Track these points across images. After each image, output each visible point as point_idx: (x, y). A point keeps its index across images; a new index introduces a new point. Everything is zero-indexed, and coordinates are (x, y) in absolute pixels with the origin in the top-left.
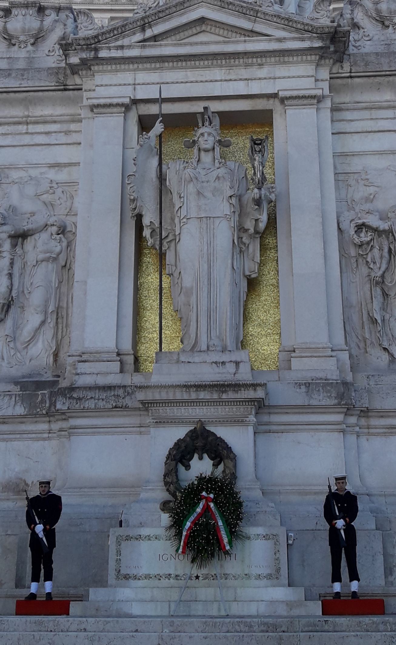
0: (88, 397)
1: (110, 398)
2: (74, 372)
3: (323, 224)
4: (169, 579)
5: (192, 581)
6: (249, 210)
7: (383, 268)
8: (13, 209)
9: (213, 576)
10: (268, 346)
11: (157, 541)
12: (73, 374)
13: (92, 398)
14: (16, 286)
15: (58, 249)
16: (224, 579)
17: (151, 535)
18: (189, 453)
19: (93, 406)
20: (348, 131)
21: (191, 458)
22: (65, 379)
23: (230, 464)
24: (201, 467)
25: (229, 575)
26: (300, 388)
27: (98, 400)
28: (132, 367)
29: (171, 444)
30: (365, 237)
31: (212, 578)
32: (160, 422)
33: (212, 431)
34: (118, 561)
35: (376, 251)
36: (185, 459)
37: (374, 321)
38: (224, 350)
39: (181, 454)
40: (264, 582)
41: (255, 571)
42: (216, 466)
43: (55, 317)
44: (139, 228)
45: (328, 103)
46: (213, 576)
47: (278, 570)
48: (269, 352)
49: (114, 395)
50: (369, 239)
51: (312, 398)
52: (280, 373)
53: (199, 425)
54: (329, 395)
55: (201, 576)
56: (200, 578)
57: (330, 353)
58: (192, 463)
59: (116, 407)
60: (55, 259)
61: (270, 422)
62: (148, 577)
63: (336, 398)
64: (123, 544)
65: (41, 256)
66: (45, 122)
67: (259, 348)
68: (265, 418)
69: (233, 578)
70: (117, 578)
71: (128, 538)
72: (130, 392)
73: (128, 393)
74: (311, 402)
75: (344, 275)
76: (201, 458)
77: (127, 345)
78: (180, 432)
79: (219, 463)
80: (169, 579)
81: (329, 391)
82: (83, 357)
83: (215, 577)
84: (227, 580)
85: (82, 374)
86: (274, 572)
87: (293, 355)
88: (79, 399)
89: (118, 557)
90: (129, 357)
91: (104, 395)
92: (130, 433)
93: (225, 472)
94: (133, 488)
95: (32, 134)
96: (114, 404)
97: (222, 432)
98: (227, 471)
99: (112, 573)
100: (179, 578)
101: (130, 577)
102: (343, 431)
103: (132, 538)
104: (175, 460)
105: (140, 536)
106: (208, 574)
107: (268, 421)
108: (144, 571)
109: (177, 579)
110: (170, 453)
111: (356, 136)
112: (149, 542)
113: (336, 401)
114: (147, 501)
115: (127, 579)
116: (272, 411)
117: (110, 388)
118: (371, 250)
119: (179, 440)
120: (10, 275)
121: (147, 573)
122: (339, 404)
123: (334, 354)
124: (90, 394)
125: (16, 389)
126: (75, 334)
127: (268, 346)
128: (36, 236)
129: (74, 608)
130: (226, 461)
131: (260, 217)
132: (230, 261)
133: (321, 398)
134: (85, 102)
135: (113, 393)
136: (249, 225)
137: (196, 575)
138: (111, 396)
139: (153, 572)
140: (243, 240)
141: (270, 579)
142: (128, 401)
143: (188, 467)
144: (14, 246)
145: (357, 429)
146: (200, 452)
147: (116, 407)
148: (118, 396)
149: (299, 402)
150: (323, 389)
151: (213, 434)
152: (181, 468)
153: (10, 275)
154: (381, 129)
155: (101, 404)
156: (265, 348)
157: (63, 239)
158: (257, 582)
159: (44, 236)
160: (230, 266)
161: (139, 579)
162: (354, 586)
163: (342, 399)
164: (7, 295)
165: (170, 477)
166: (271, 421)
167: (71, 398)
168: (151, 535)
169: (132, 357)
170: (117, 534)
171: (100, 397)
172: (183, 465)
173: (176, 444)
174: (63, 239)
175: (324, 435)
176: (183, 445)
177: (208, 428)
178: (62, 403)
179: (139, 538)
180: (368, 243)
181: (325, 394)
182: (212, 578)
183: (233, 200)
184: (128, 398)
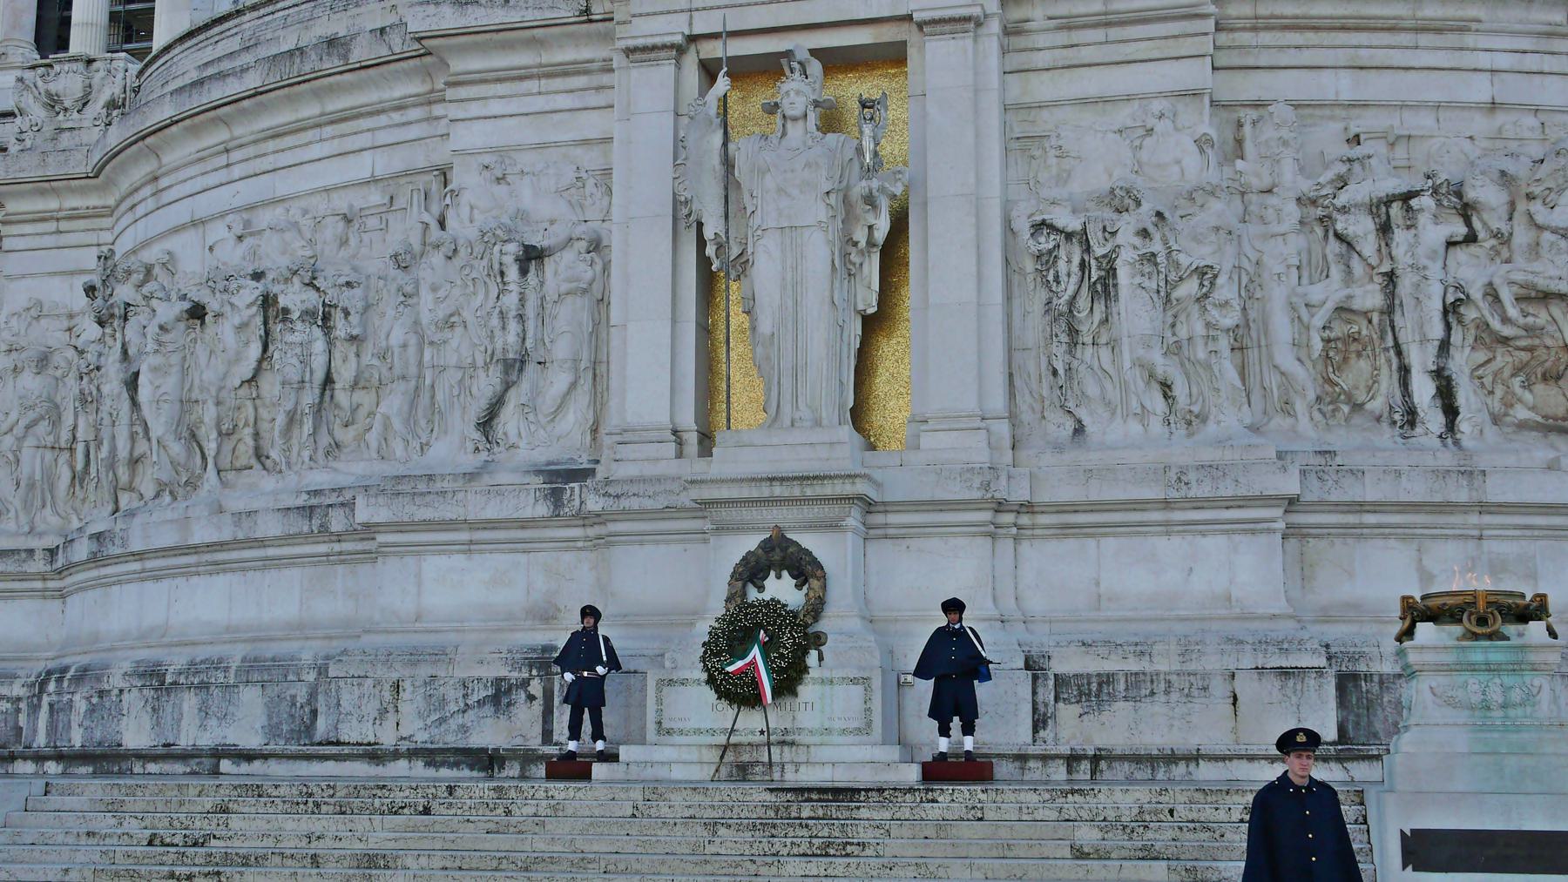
3: (978, 227)
6: (859, 211)
7: (1070, 292)
8: (521, 215)
14: (530, 334)
15: (589, 274)
20: (1032, 66)
24: (781, 589)
30: (1046, 242)
32: (722, 529)
35: (1062, 266)
37: (1055, 373)
38: (818, 423)
39: (752, 571)
40: (850, 739)
41: (838, 725)
42: (799, 587)
43: (590, 375)
44: (701, 243)
45: (995, 26)
47: (869, 724)
50: (1051, 246)
57: (978, 423)
60: (585, 291)
64: (666, 690)
65: (564, 287)
66: (566, 74)
68: (878, 519)
71: (671, 682)
75: (1016, 302)
76: (779, 577)
77: (687, 419)
78: (751, 542)
82: (626, 436)
88: (617, 496)
92: (690, 541)
95: (547, 93)
97: (807, 541)
99: (651, 727)
102: (993, 536)
108: (693, 724)
111: (1046, 76)
117: (659, 480)
118: (1055, 262)
120: (521, 318)
123: (983, 424)
124: (634, 489)
125: (537, 482)
126: (613, 403)
128: (557, 256)
129: (599, 770)
131: (872, 221)
132: (827, 293)
134: (622, 44)
136: (861, 236)
140: (852, 257)
143: (761, 589)
144: (524, 272)
145: (1014, 530)
153: (521, 318)
154: (1086, 61)
155: (649, 504)
157: (597, 260)
158: (841, 739)
159: (567, 257)
160: (828, 300)
162: (969, 743)
164: (518, 348)
173: (744, 559)
174: (597, 260)
175: (961, 541)
179: (684, 682)
180: (1050, 252)
183: (833, 199)
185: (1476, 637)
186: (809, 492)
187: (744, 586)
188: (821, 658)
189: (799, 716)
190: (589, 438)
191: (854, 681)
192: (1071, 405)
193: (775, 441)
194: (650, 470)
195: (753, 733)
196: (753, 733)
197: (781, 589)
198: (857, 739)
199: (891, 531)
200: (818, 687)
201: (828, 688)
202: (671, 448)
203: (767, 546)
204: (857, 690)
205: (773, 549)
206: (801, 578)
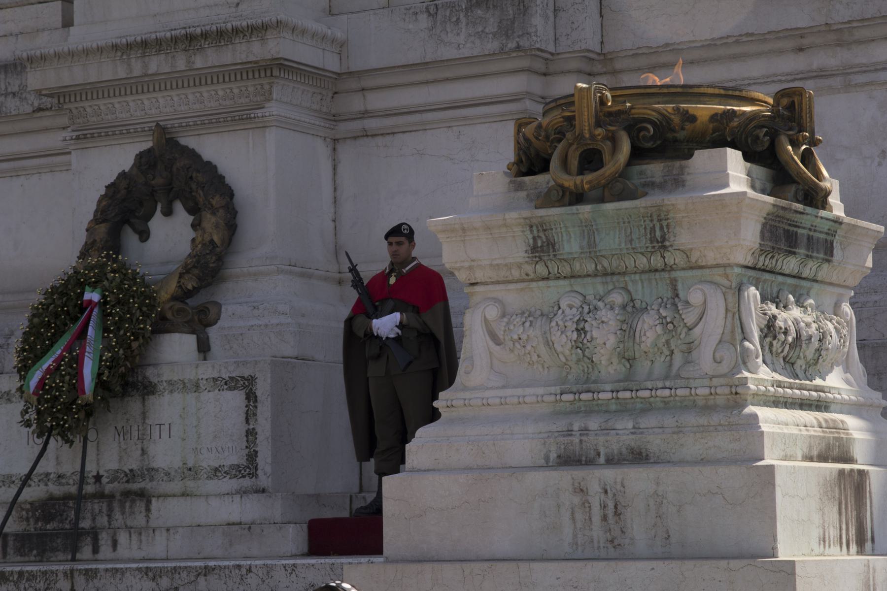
4: (46, 485)
9: (126, 475)
25: (157, 470)
26: (416, 20)
41: (209, 461)
47: (252, 457)
54: (480, 29)
55: (106, 474)
56: (104, 480)
59: (40, 109)
61: (366, 112)
63: (494, 35)
68: (356, 104)
76: (168, 212)
80: (46, 485)
84: (155, 483)
86: (244, 462)
96: (36, 104)
100: (64, 481)
106: (117, 471)
107: (362, 108)
109: (60, 484)
116: (368, 82)
119: (123, 175)
122: (502, 51)
133: (461, 39)
137: (95, 474)
141: (235, 476)
143: (144, 235)
147: (40, 109)
149: (414, 57)
150: (466, 16)
151: (193, 155)
158: (213, 486)
166: (370, 107)
171: (9, 90)
172: (135, 230)
177: (183, 141)
182: (125, 479)
185: (578, 198)
186: (199, 62)
188: (204, 348)
189: (152, 449)
191: (231, 384)
199: (372, 124)
200: (177, 396)
201: (191, 398)
203: (146, 161)
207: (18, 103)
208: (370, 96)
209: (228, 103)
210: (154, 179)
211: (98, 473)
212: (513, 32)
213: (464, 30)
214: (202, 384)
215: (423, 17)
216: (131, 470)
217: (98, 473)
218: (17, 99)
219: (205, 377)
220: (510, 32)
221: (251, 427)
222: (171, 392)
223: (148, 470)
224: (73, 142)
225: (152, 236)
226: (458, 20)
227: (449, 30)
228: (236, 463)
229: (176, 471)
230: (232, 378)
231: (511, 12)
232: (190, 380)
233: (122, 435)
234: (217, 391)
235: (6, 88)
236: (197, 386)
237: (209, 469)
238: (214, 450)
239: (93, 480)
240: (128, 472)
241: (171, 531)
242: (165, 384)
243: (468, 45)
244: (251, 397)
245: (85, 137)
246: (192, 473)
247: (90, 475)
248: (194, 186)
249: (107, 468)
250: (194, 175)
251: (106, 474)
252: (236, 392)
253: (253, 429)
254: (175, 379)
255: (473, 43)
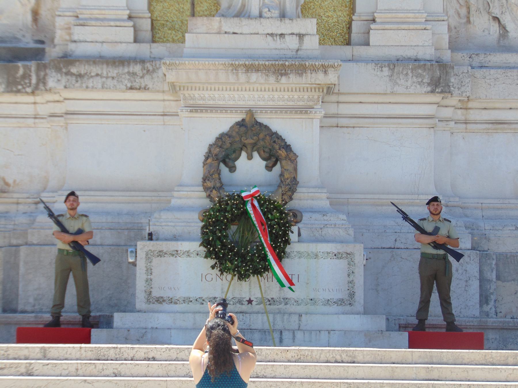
0: (93, 74)
1: (123, 76)
2: (67, 38)
5: (243, 306)
9: (269, 301)
10: (335, 11)
11: (198, 257)
12: (67, 40)
13: (97, 75)
16: (283, 304)
17: (192, 251)
18: (234, 152)
19: (100, 86)
21: (237, 158)
22: (55, 46)
23: (289, 166)
25: (290, 299)
26: (382, 71)
27: (107, 78)
28: (148, 35)
29: (211, 139)
31: (268, 303)
32: (195, 109)
33: (265, 124)
34: (149, 281)
36: (229, 159)
38: (283, 16)
39: (224, 153)
40: (335, 308)
42: (269, 168)
46: (269, 301)
47: (352, 295)
48: (335, 20)
49: (129, 73)
51: (397, 83)
52: (355, 50)
53: (249, 115)
54: (420, 80)
55: (255, 300)
56: (254, 303)
58: (238, 163)
61: (338, 114)
62: (187, 300)
64: (156, 261)
67: (322, 14)
69: (295, 304)
70: (148, 301)
71: (161, 254)
72: (151, 68)
73: (148, 71)
74: (395, 89)
76: (250, 157)
79: (275, 164)
81: (418, 76)
83: (272, 302)
84: (288, 306)
85: (80, 42)
87: (373, 26)
88: (80, 76)
89: (149, 277)
90: (144, 20)
91: (114, 72)
93: (283, 176)
94: (161, 194)
96: (129, 85)
97: (277, 124)
98: (287, 175)
101: (164, 301)
103: (166, 254)
104: (217, 159)
105: (177, 251)
107: (336, 112)
108: (181, 293)
110: (210, 151)
112: (189, 258)
113: (429, 89)
114: (180, 209)
115: (161, 303)
116: (342, 98)
121: (186, 295)
124: (95, 70)
127: (335, 11)
130: (284, 162)
133: (409, 83)
135: (126, 70)
137: (248, 299)
138: (124, 74)
139: (193, 294)
141: (341, 305)
142: (147, 81)
143: (232, 169)
146: (249, 151)
147: (131, 88)
148: (134, 74)
150: (412, 72)
152: (224, 169)
156: (330, 14)
158: (326, 309)
161: (176, 303)
163: (436, 86)
165: (211, 180)
166: (340, 112)
167: (68, 73)
168: (192, 251)
169: (149, 21)
170: (146, 249)
171: (110, 75)
176: (228, 141)
177: (259, 120)
178: (56, 80)
179: (175, 254)
181: (415, 79)
182: (268, 303)
184: (147, 77)
187: (219, 164)
190: (29, 18)
192: (496, 12)
193: (246, 30)
194: (107, 50)
195: (240, 302)
196: (240, 302)
197: (250, 172)
198: (340, 309)
199: (343, 122)
202: (128, 34)
204: (343, 264)
205: (246, 133)
206: (272, 159)
207: (116, 84)
208: (341, 105)
209: (301, 103)
210: (246, 139)
211: (250, 299)
212: (440, 83)
213: (410, 79)
214: (320, 255)
215: (386, 69)
216: (272, 299)
217: (250, 299)
218: (115, 81)
219: (322, 251)
220: (438, 84)
221: (351, 279)
222: (300, 258)
223: (284, 299)
224: (187, 113)
225: (237, 170)
226: (407, 74)
227: (401, 78)
228: (341, 297)
229: (302, 300)
230: (339, 253)
231: (439, 74)
232: (312, 252)
233: (266, 279)
234: (329, 259)
235: (107, 74)
236: (317, 255)
237: (324, 300)
238: (327, 290)
239: (247, 303)
240: (270, 299)
241: (332, 332)
242: (295, 253)
243: (412, 87)
244: (351, 263)
245: (196, 111)
246: (312, 302)
247: (245, 300)
248: (277, 147)
249: (256, 297)
250: (277, 140)
251: (255, 300)
252: (341, 260)
253: (353, 280)
254: (302, 251)
255: (416, 86)
